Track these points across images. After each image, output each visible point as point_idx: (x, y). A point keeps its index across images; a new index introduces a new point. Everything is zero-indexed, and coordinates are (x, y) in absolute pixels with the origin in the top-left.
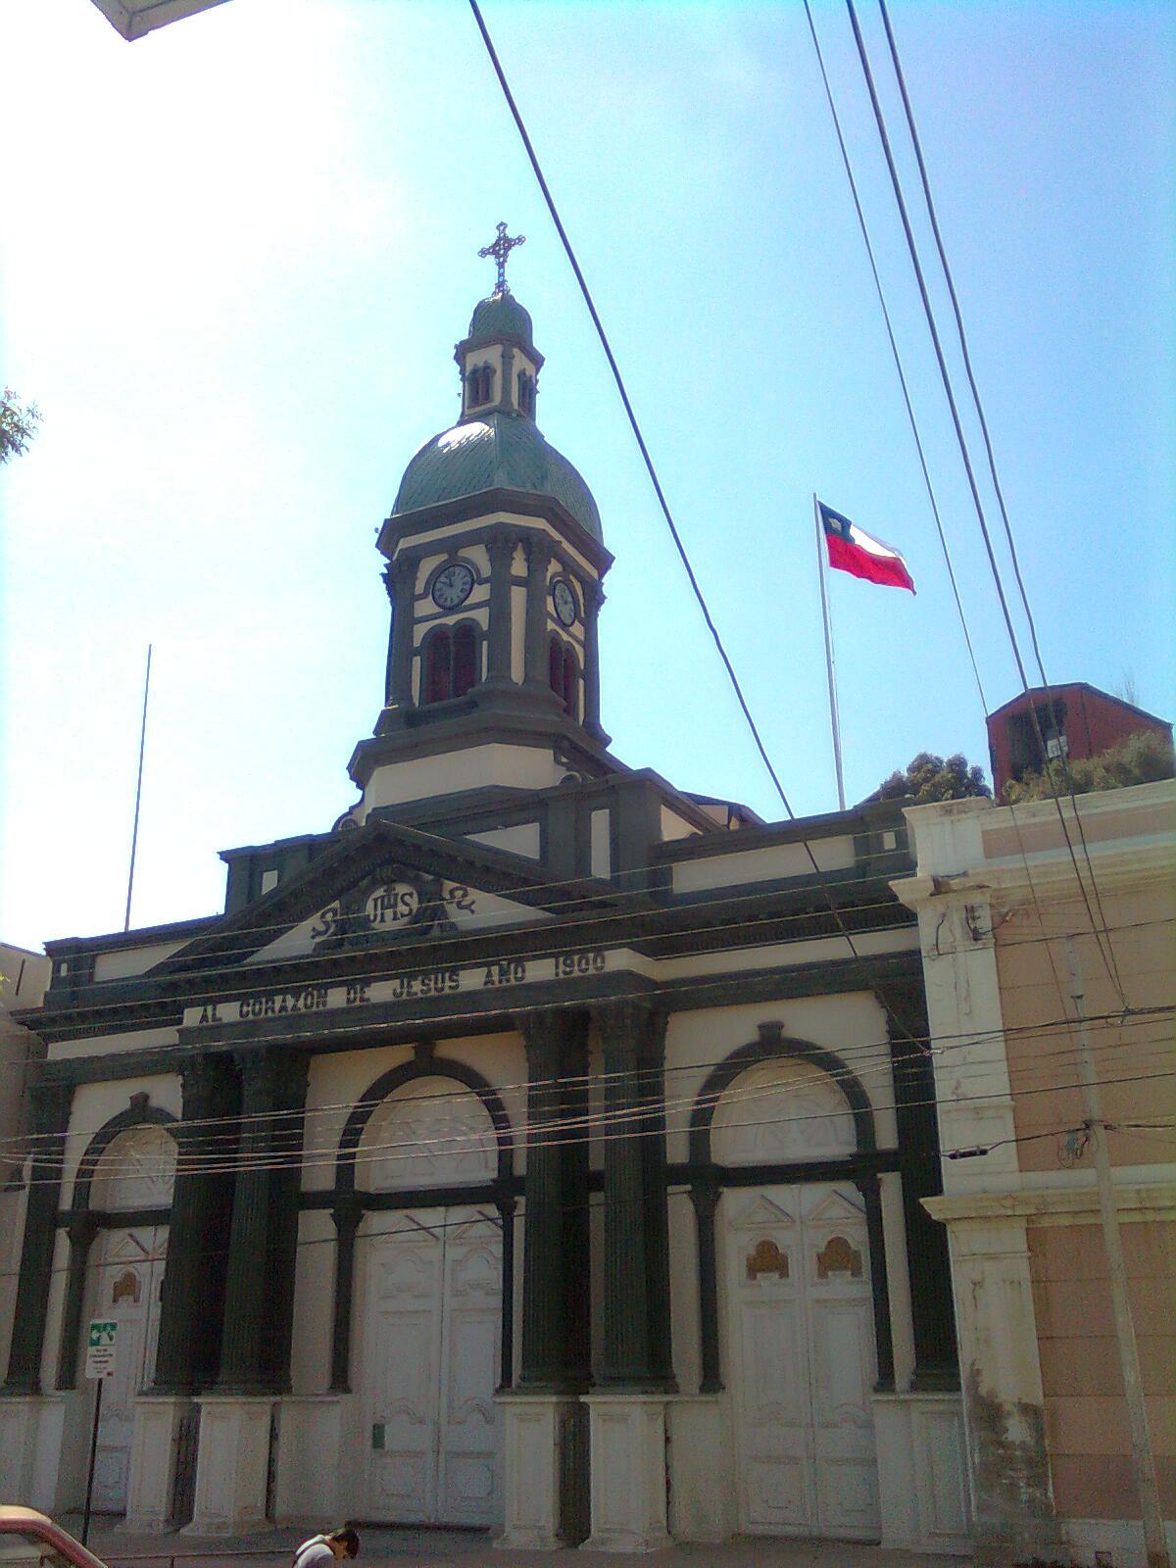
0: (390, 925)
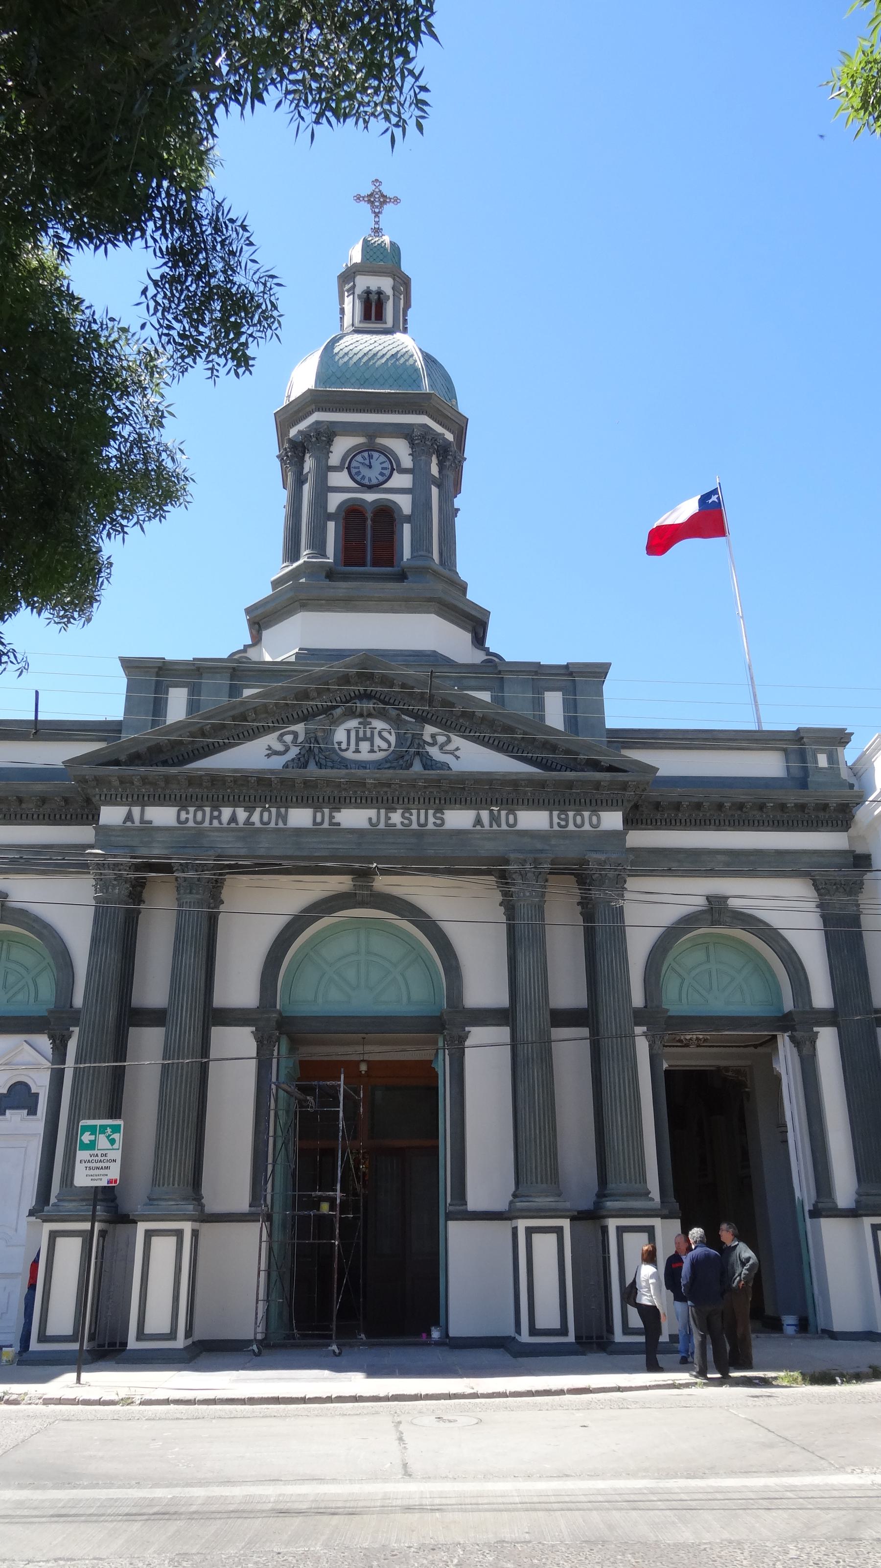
0: (365, 754)
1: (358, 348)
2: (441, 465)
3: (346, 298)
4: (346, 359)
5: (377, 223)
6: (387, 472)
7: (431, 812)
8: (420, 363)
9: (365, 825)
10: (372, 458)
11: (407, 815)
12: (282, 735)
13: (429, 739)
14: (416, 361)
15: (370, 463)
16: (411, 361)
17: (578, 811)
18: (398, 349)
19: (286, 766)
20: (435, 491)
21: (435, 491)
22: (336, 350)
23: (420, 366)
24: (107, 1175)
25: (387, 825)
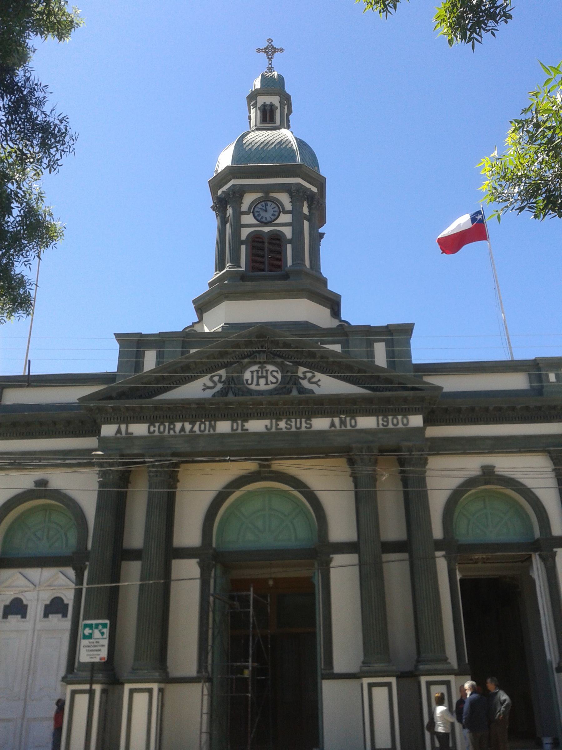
0: (262, 386)
1: (258, 139)
2: (310, 207)
3: (252, 110)
4: (250, 146)
5: (270, 64)
6: (276, 214)
7: (303, 420)
8: (295, 146)
9: (263, 429)
10: (267, 205)
11: (289, 422)
12: (212, 377)
13: (301, 375)
14: (292, 145)
15: (266, 208)
16: (290, 146)
17: (395, 416)
18: (282, 138)
19: (214, 396)
20: (306, 223)
21: (306, 223)
22: (244, 142)
23: (295, 148)
24: (99, 655)
25: (277, 429)
